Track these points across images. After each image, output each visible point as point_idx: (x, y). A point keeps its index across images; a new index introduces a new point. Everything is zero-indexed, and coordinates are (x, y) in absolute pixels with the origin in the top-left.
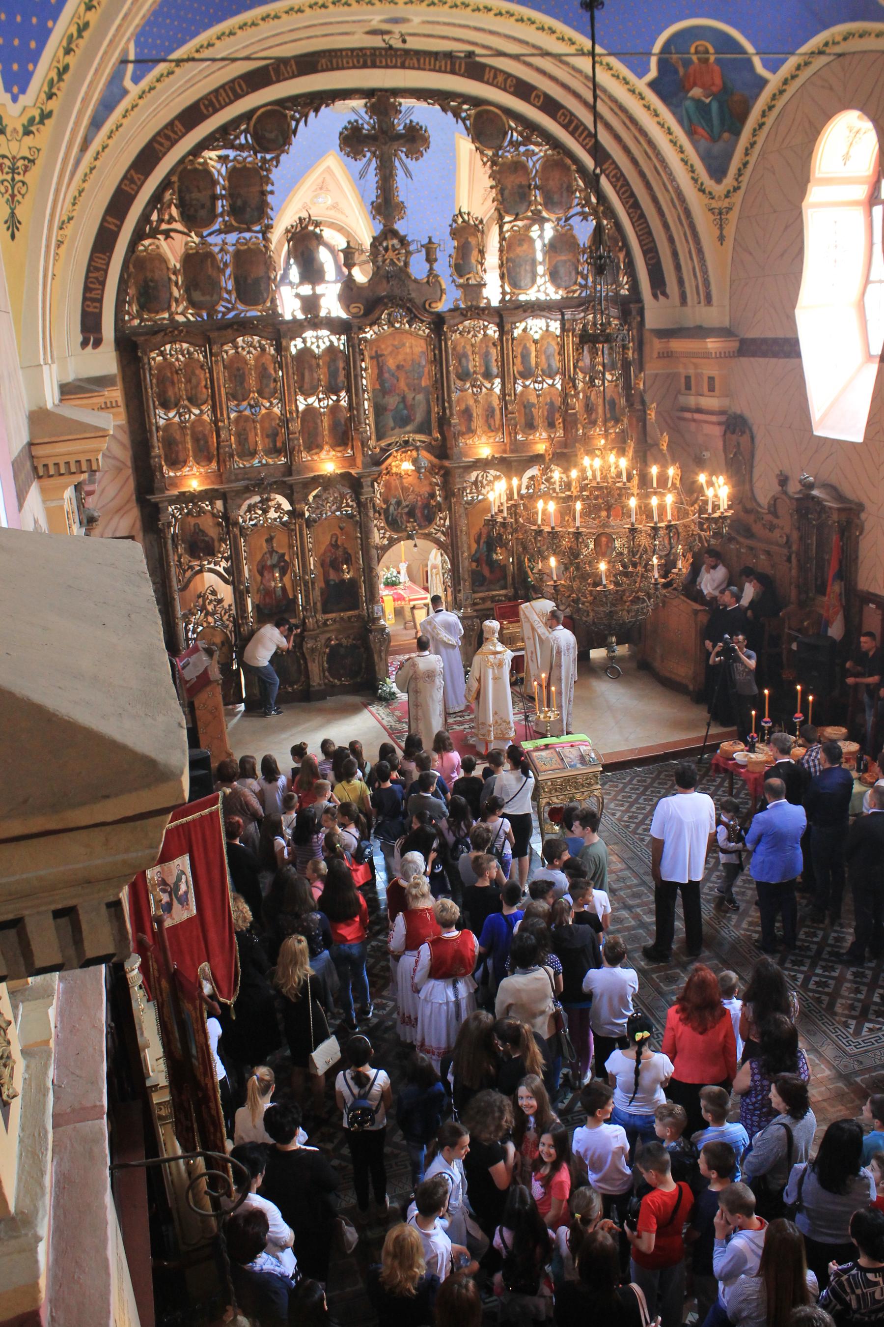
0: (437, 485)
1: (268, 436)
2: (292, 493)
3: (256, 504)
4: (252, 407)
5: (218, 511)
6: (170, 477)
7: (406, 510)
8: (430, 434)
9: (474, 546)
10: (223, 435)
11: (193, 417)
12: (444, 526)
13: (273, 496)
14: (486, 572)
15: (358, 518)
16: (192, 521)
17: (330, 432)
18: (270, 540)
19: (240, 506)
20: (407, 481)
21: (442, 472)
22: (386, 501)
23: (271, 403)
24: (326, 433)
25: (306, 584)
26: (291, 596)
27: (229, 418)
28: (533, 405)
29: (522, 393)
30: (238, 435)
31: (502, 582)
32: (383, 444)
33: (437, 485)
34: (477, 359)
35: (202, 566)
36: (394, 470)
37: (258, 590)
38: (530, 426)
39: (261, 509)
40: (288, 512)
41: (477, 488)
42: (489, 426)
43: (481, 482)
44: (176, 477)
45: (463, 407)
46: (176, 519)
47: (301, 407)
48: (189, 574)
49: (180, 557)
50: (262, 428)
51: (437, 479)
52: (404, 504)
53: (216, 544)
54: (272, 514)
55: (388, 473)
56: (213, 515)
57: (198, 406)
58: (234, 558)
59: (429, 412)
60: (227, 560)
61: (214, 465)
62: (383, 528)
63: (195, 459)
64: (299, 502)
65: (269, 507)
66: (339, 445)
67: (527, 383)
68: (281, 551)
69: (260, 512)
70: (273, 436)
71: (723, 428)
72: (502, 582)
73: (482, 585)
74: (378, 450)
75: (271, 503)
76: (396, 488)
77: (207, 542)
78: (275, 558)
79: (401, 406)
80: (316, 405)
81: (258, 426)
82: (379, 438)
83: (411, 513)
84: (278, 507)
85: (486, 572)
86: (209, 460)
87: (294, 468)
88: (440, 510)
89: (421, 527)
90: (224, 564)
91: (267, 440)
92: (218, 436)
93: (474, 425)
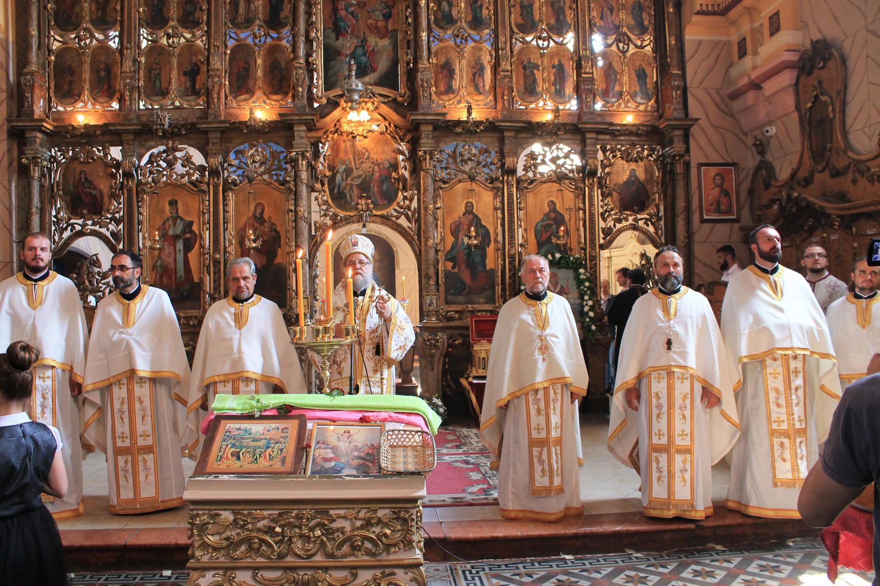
0: (402, 153)
1: (185, 74)
2: (207, 143)
3: (160, 153)
4: (169, 36)
5: (113, 159)
6: (59, 111)
7: (358, 181)
8: (394, 86)
9: (450, 240)
10: (128, 65)
11: (95, 42)
12: (409, 208)
13: (186, 146)
14: (466, 277)
15: (292, 185)
16: (78, 168)
17: (264, 74)
18: (173, 203)
19: (140, 158)
20: (361, 143)
21: (409, 137)
22: (331, 168)
23: (194, 35)
24: (260, 73)
25: (217, 263)
26: (196, 280)
27: (139, 47)
28: (536, 66)
29: (522, 50)
30: (149, 70)
31: (488, 293)
32: (332, 94)
33: (402, 153)
34: (463, 5)
35: (83, 226)
36: (346, 128)
37: (154, 267)
38: (530, 91)
39: (164, 161)
40: (202, 169)
41: (455, 162)
42: (476, 87)
43: (461, 155)
44: (66, 112)
45: (443, 60)
46: (59, 163)
47: (231, 43)
48: (67, 234)
49: (58, 213)
50: (179, 63)
51: (403, 147)
52: (355, 173)
53: (106, 200)
54: (179, 168)
55: (336, 131)
56: (107, 165)
57: (104, 31)
58: (129, 220)
59: (395, 62)
60: (118, 222)
61: (115, 105)
62: (326, 203)
63: (92, 91)
64: (215, 154)
65: (176, 158)
66: (276, 93)
67: (528, 39)
68: (189, 219)
69: (164, 165)
70: (192, 73)
71: (795, 73)
72: (488, 293)
73: (460, 294)
74: (324, 101)
75: (179, 154)
76: (346, 152)
77: (94, 196)
78: (179, 229)
79: (360, 51)
80: (250, 41)
81: (175, 62)
82: (329, 85)
83: (364, 188)
84: (187, 160)
85: (466, 277)
86: (111, 98)
87: (211, 111)
88: (405, 189)
89: (377, 206)
90: (112, 227)
91: (183, 78)
92: (121, 67)
93: (456, 84)
